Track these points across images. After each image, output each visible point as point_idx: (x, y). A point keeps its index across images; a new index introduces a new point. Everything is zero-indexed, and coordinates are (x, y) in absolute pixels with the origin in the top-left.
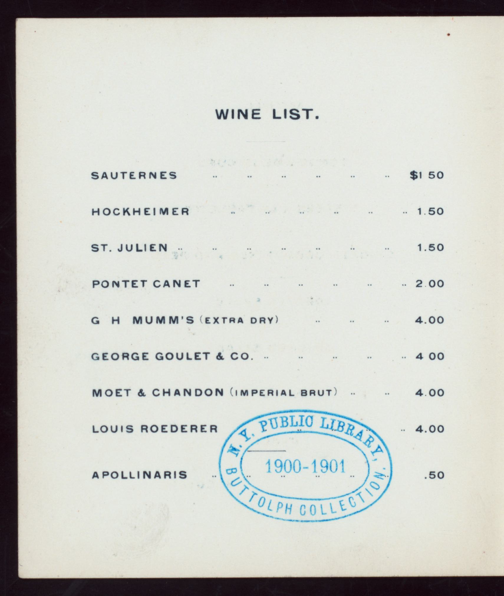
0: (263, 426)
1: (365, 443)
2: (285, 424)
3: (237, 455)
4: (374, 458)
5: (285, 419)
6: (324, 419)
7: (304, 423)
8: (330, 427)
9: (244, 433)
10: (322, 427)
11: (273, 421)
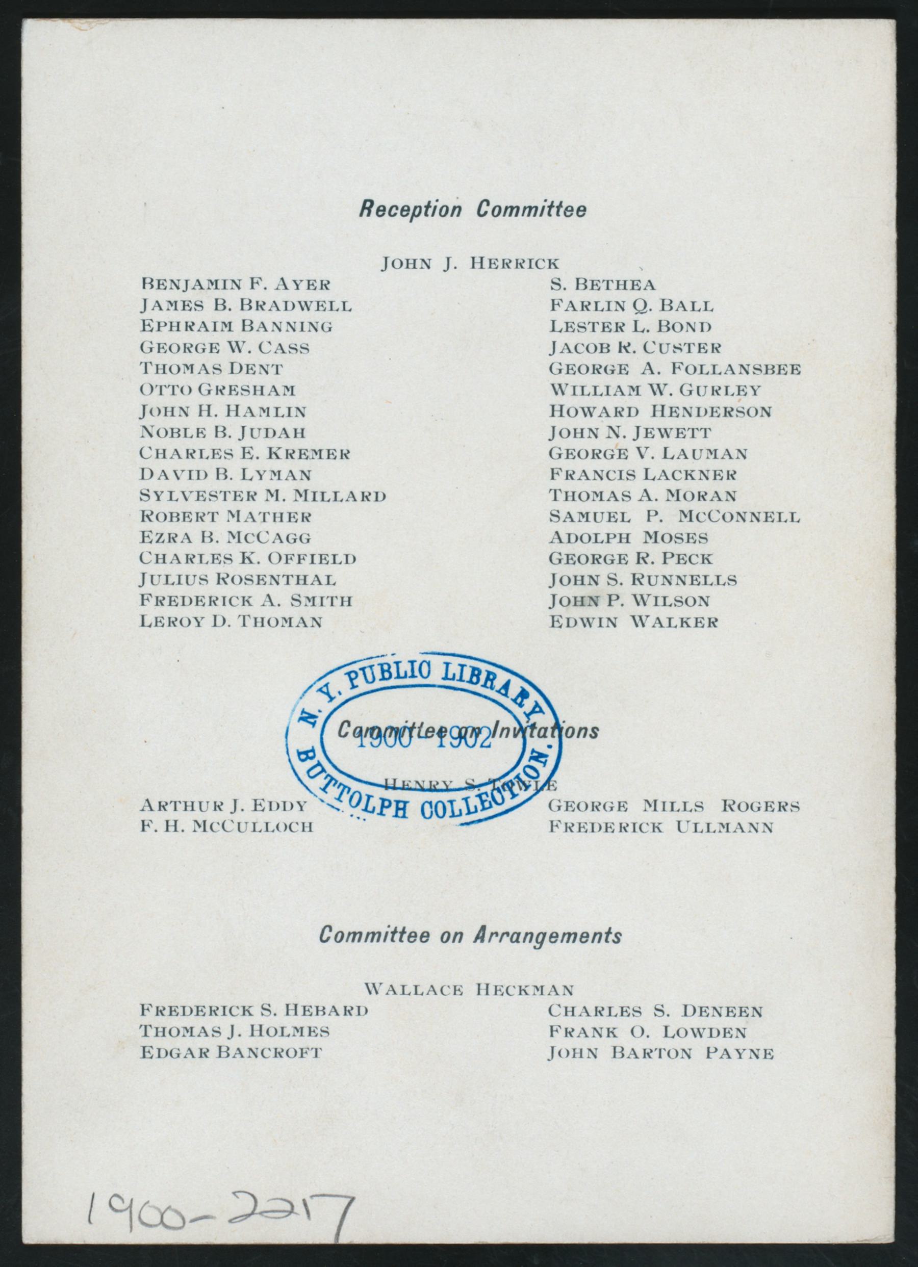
0: (351, 680)
1: (515, 701)
2: (387, 675)
3: (314, 724)
5: (386, 667)
6: (447, 664)
7: (417, 673)
8: (458, 677)
9: (324, 691)
11: (368, 671)
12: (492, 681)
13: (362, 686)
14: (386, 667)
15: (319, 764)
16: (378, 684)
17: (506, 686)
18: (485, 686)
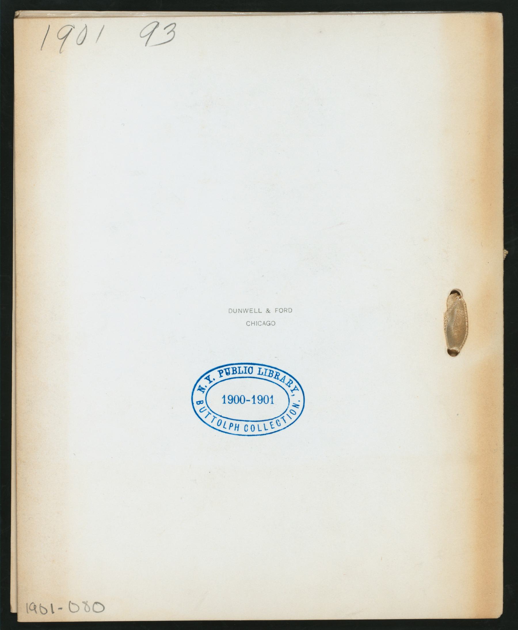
0: (220, 374)
2: (235, 372)
3: (203, 392)
5: (234, 369)
7: (247, 372)
8: (264, 374)
9: (208, 378)
10: (259, 374)
13: (225, 376)
16: (231, 376)
18: (275, 378)
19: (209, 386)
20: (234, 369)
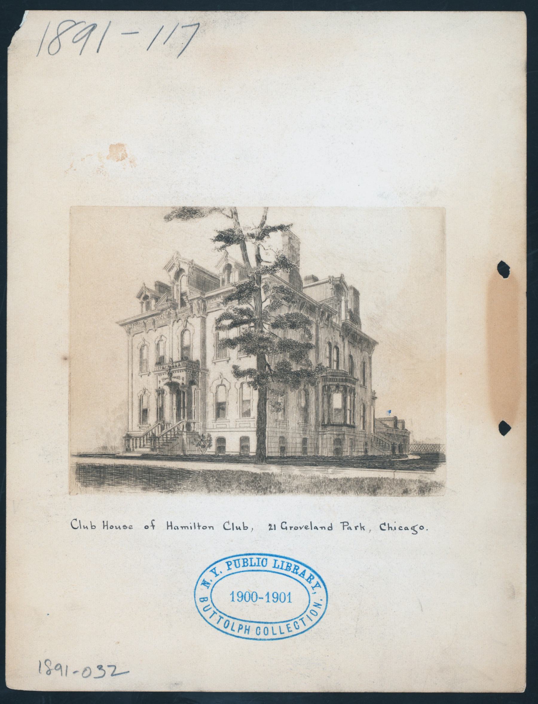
0: (229, 565)
1: (307, 580)
3: (208, 587)
4: (313, 592)
6: (276, 561)
7: (260, 564)
8: (280, 567)
9: (214, 571)
10: (274, 567)
11: (237, 562)
12: (297, 570)
13: (234, 569)
14: (245, 560)
15: (235, 561)
16: (241, 569)
17: (303, 573)
19: (216, 579)
20: (245, 560)
